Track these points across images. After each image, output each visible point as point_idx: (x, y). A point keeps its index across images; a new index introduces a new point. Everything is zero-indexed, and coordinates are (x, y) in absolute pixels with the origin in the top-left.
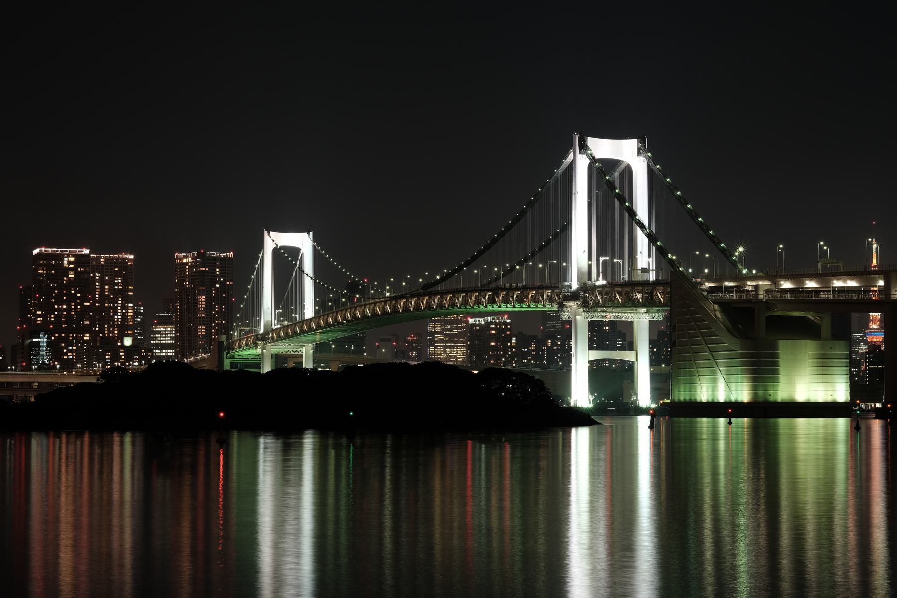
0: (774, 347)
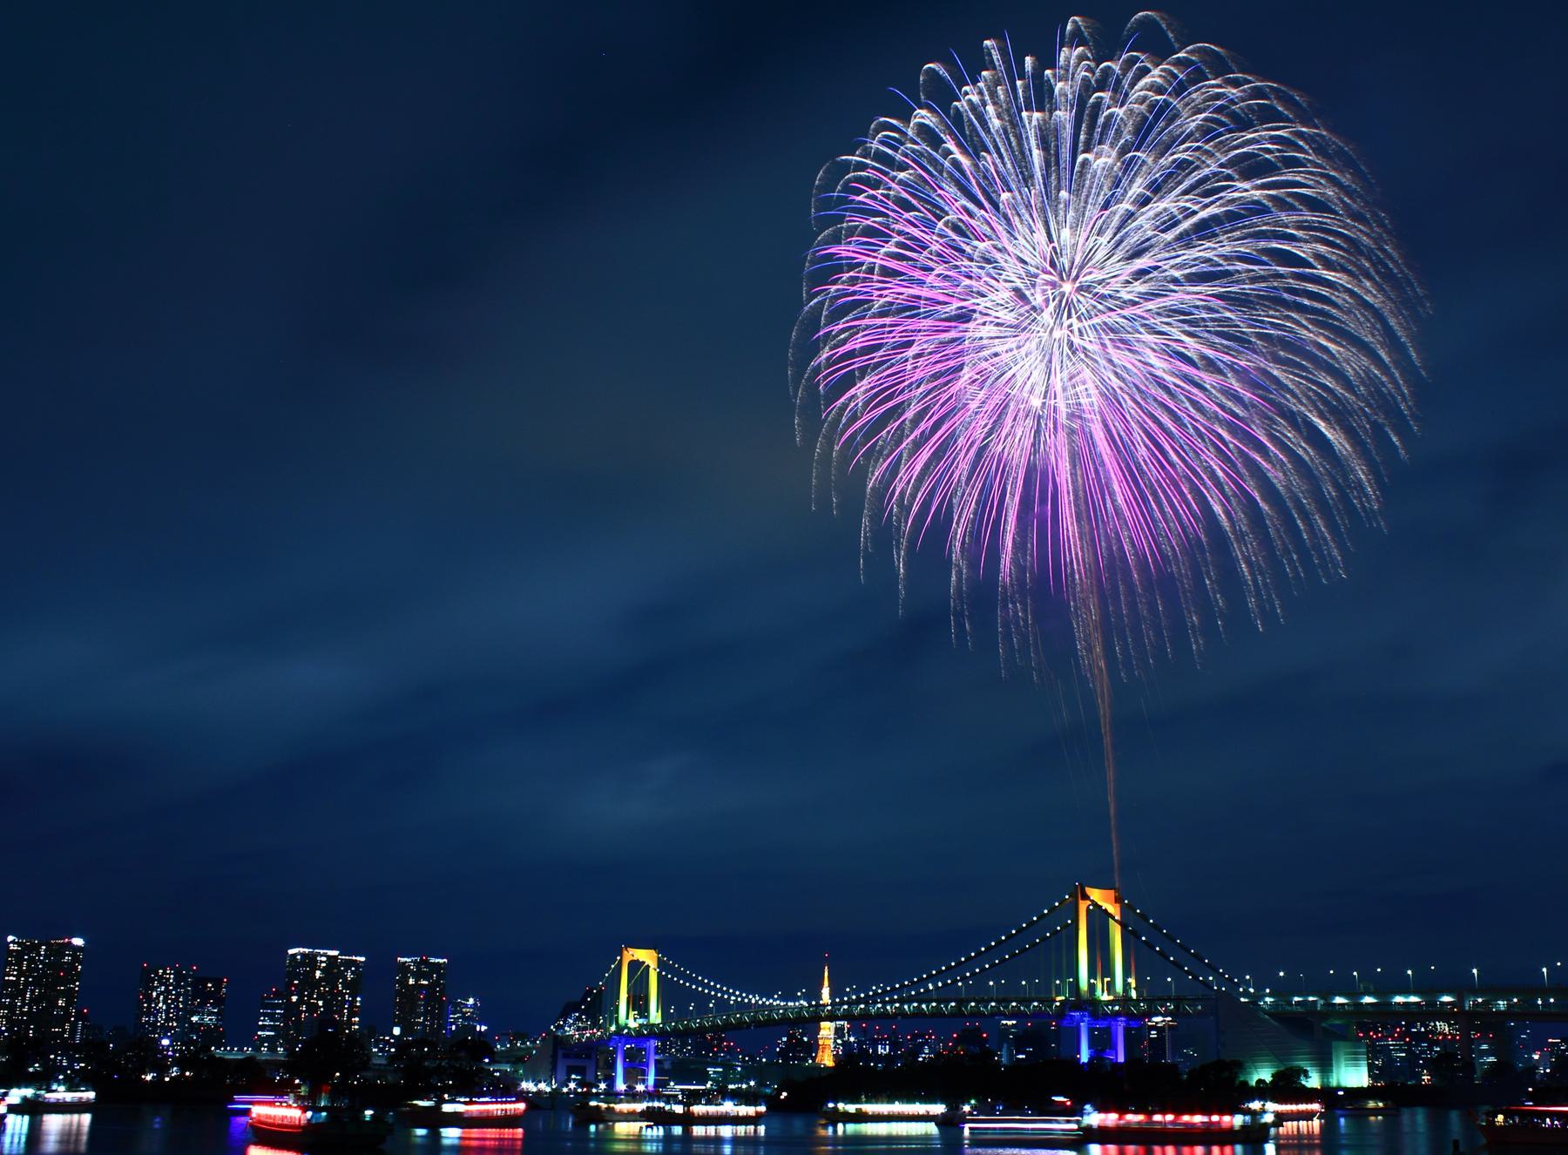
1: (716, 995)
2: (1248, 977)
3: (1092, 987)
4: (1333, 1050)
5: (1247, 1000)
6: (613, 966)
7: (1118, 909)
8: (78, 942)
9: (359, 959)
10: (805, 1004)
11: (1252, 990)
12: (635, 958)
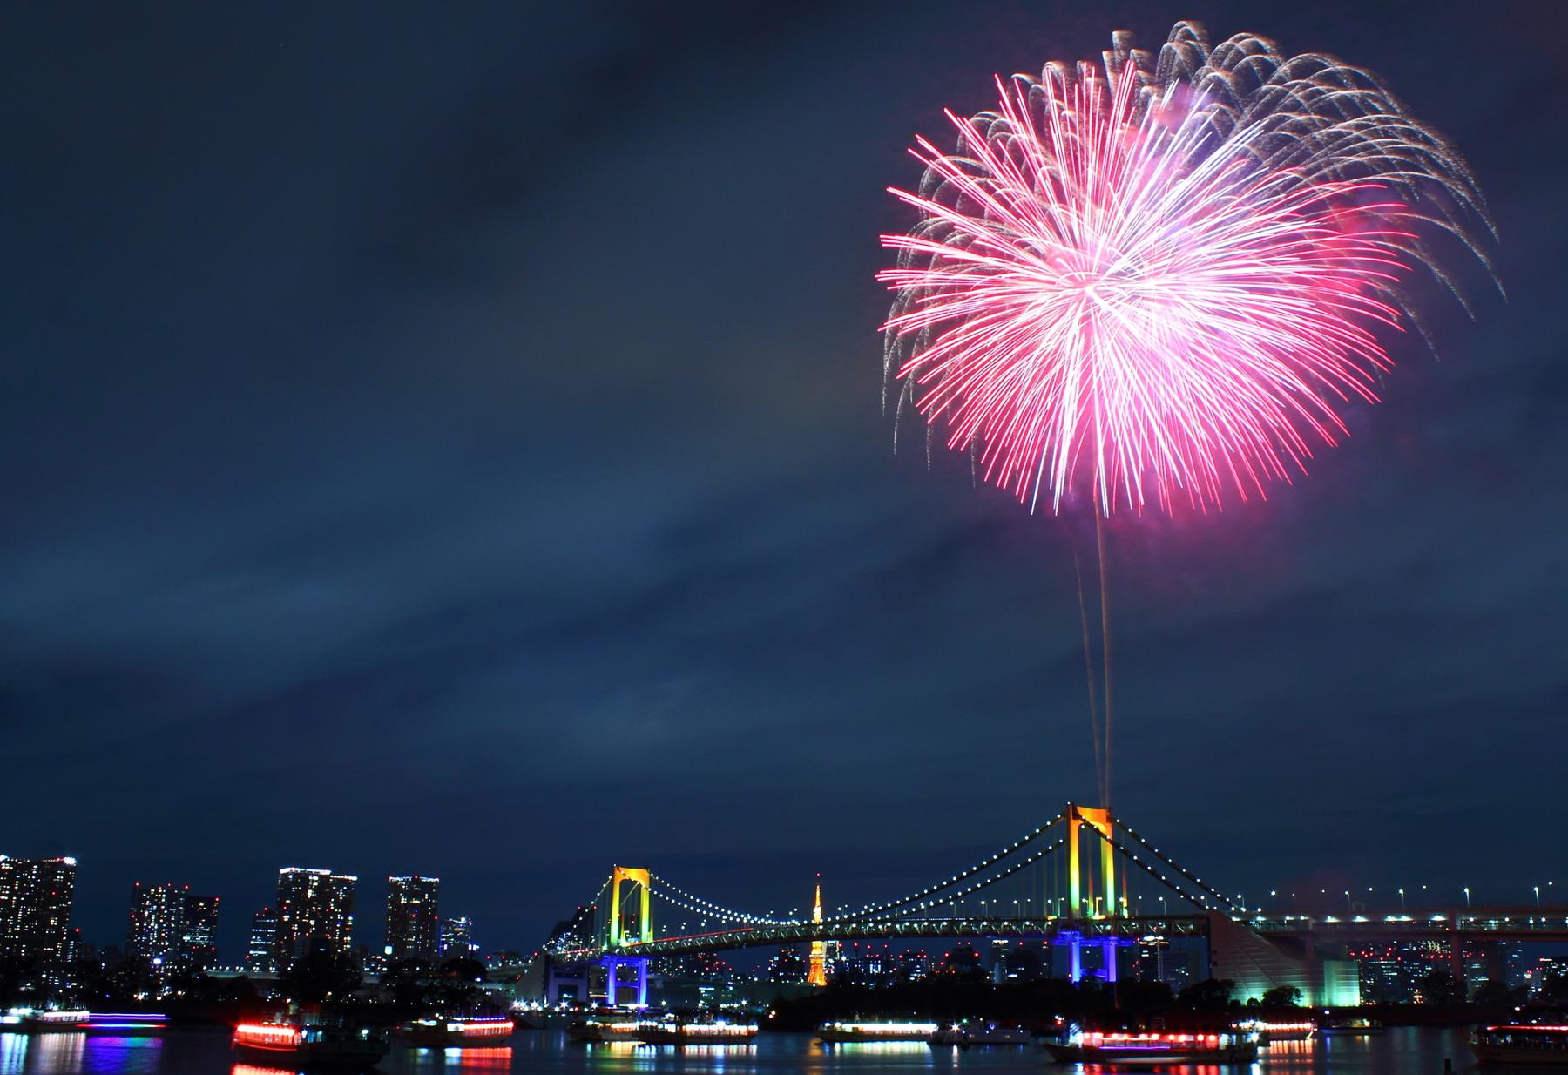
0: (1322, 966)
1: (708, 914)
2: (1239, 897)
3: (1084, 907)
4: (1325, 970)
5: (1238, 920)
6: (605, 886)
7: (1110, 828)
8: (70, 861)
9: (350, 878)
10: (797, 923)
11: (1243, 910)
12: (627, 878)
